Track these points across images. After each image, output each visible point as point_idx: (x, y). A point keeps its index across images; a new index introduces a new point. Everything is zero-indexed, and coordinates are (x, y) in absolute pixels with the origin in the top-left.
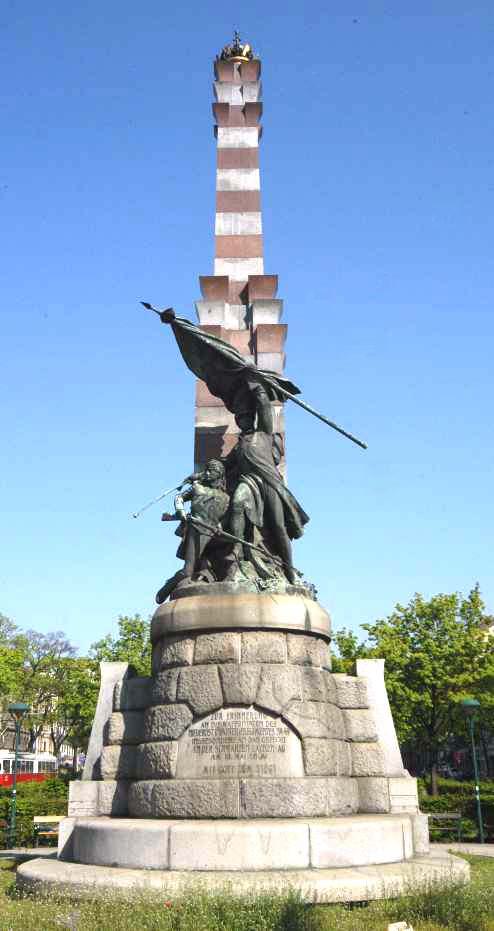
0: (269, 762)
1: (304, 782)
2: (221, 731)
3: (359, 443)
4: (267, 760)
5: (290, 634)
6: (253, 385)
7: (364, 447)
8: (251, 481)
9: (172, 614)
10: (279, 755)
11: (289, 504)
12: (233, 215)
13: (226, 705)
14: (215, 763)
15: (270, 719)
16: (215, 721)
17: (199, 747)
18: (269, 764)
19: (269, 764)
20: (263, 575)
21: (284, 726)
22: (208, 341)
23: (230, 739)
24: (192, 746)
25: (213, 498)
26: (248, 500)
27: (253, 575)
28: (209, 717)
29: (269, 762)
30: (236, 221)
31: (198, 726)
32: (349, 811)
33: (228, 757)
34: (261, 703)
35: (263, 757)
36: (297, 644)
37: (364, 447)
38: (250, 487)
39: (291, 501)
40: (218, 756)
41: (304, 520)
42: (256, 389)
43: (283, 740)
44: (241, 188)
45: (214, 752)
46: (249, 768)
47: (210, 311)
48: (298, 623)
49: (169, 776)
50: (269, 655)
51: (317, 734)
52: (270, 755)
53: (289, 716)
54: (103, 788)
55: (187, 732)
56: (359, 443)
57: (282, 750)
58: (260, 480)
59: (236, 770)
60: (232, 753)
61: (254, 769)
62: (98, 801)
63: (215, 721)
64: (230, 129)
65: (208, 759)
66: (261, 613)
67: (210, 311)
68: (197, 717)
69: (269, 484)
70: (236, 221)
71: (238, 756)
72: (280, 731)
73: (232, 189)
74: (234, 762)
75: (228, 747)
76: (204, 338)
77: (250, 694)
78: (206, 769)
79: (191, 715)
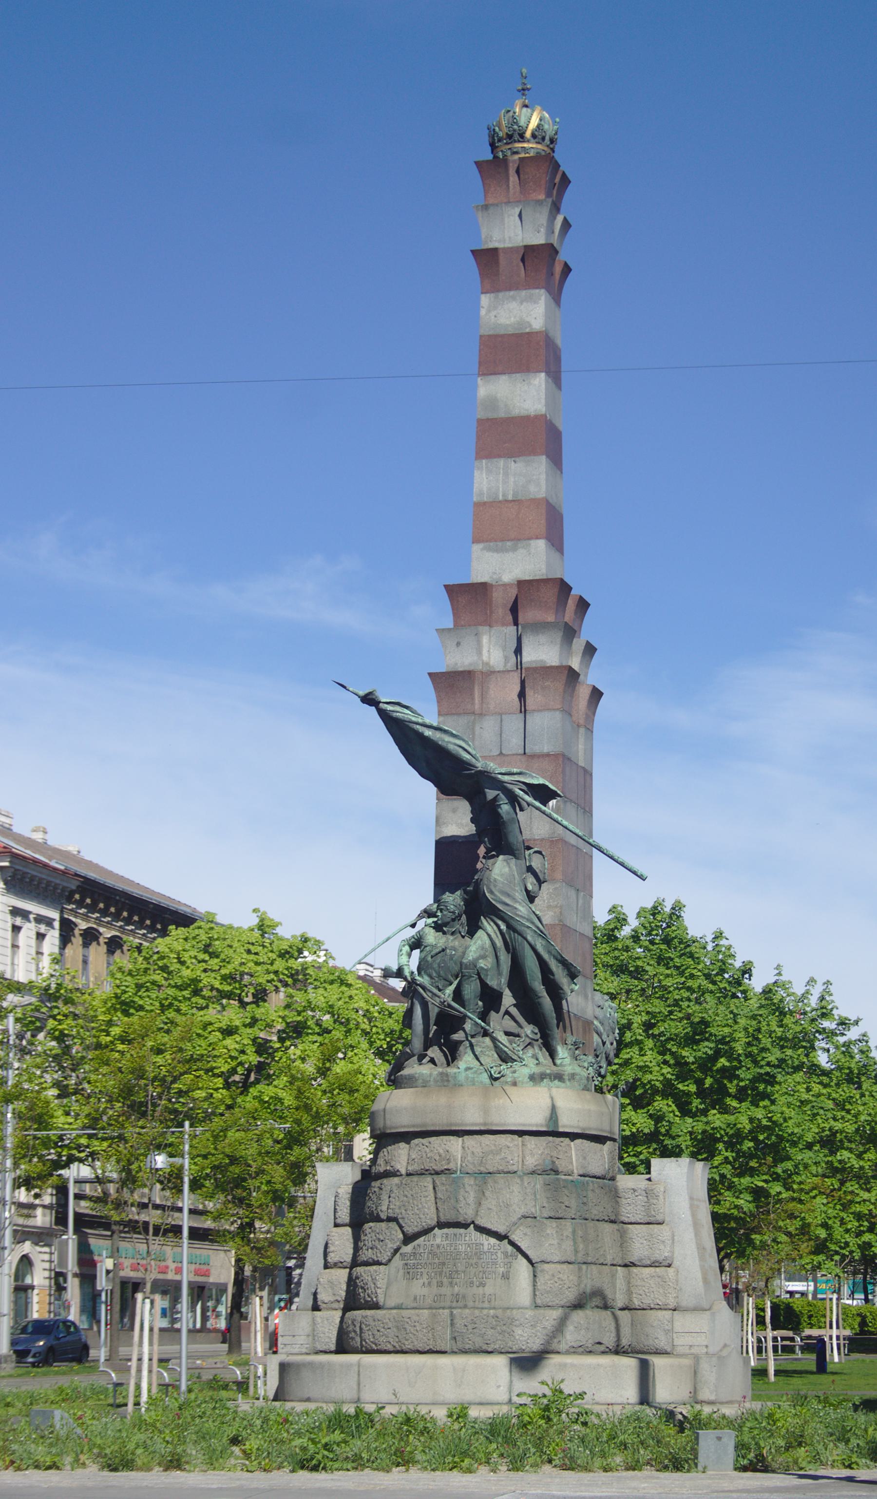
0: (488, 1290)
1: (529, 1313)
4: (486, 1288)
5: (527, 1137)
6: (491, 794)
7: (642, 878)
9: (384, 1110)
11: (546, 956)
12: (501, 462)
13: (441, 1225)
14: (425, 1291)
15: (493, 1241)
17: (408, 1273)
18: (487, 1293)
19: (487, 1293)
21: (510, 1248)
22: (428, 733)
23: (444, 1264)
24: (401, 1272)
26: (483, 957)
27: (490, 1058)
28: (422, 1239)
30: (506, 474)
31: (408, 1249)
32: (602, 1348)
33: (440, 1284)
34: (482, 1222)
36: (535, 1152)
37: (642, 878)
38: (489, 935)
39: (549, 952)
40: (429, 1283)
42: (495, 799)
43: (509, 1265)
44: (516, 412)
45: (425, 1279)
46: (464, 1297)
47: (458, 644)
48: (536, 1120)
49: (376, 1306)
50: (492, 1165)
51: (557, 1259)
52: (489, 1282)
53: (514, 1237)
54: (319, 1320)
55: (398, 1254)
57: (506, 1277)
58: (503, 927)
60: (445, 1280)
62: (313, 1335)
64: (501, 295)
66: (486, 1111)
67: (458, 644)
68: (408, 1239)
69: (515, 931)
70: (506, 474)
71: (451, 1283)
73: (502, 414)
74: (446, 1290)
75: (441, 1273)
77: (467, 1212)
78: (415, 1299)
79: (401, 1236)
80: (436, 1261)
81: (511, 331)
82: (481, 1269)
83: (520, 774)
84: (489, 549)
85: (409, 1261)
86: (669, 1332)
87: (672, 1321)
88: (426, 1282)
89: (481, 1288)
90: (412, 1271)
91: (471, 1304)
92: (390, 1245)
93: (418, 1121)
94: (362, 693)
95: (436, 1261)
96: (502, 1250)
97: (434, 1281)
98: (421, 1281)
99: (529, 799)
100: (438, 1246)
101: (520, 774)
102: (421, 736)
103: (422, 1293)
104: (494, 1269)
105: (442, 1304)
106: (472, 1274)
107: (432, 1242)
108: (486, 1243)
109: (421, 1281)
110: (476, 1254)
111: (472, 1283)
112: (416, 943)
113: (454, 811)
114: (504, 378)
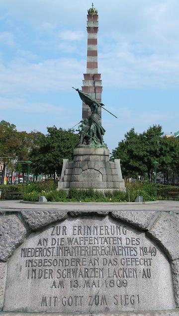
2: (64, 249)
4: (128, 287)
10: (142, 280)
14: (56, 292)
15: (131, 234)
16: (56, 237)
17: (34, 271)
18: (131, 294)
19: (131, 294)
21: (148, 244)
23: (78, 261)
24: (25, 270)
29: (131, 290)
31: (32, 243)
33: (75, 284)
35: (123, 284)
40: (61, 283)
43: (148, 262)
45: (56, 278)
46: (104, 299)
53: (156, 231)
55: (19, 251)
57: (147, 274)
59: (86, 301)
60: (81, 280)
61: (111, 300)
63: (56, 237)
65: (85, 178)
68: (32, 231)
71: (87, 283)
72: (144, 250)
74: (84, 292)
75: (75, 272)
78: (44, 300)
79: (24, 230)
80: (69, 257)
82: (121, 267)
85: (34, 258)
88: (57, 281)
89: (123, 288)
90: (38, 268)
91: (112, 307)
92: (10, 240)
95: (69, 257)
96: (141, 245)
97: (67, 281)
98: (51, 280)
100: (70, 240)
103: (53, 295)
104: (134, 267)
105: (79, 307)
106: (112, 271)
107: (61, 236)
108: (124, 237)
109: (51, 280)
110: (114, 249)
111: (112, 282)
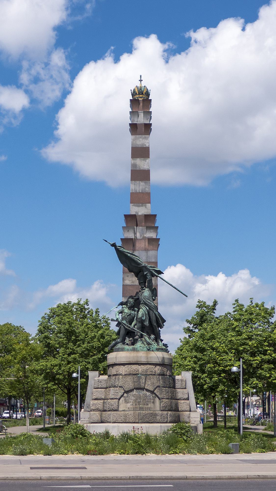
0: (149, 406)
1: (160, 412)
3: (185, 295)
7: (187, 296)
8: (144, 308)
9: (116, 357)
10: (152, 404)
12: (138, 182)
20: (149, 344)
22: (129, 255)
24: (124, 401)
25: (130, 314)
29: (149, 406)
30: (139, 186)
37: (187, 296)
41: (164, 321)
43: (154, 400)
44: (142, 168)
56: (185, 295)
57: (153, 403)
58: (148, 308)
67: (128, 231)
69: (151, 309)
70: (139, 186)
73: (138, 169)
76: (127, 254)
77: (142, 385)
81: (140, 146)
83: (154, 267)
84: (135, 206)
86: (189, 417)
87: (190, 414)
92: (120, 394)
93: (128, 360)
94: (112, 243)
99: (156, 274)
101: (154, 267)
102: (127, 256)
112: (121, 312)
113: (128, 276)
114: (138, 159)
